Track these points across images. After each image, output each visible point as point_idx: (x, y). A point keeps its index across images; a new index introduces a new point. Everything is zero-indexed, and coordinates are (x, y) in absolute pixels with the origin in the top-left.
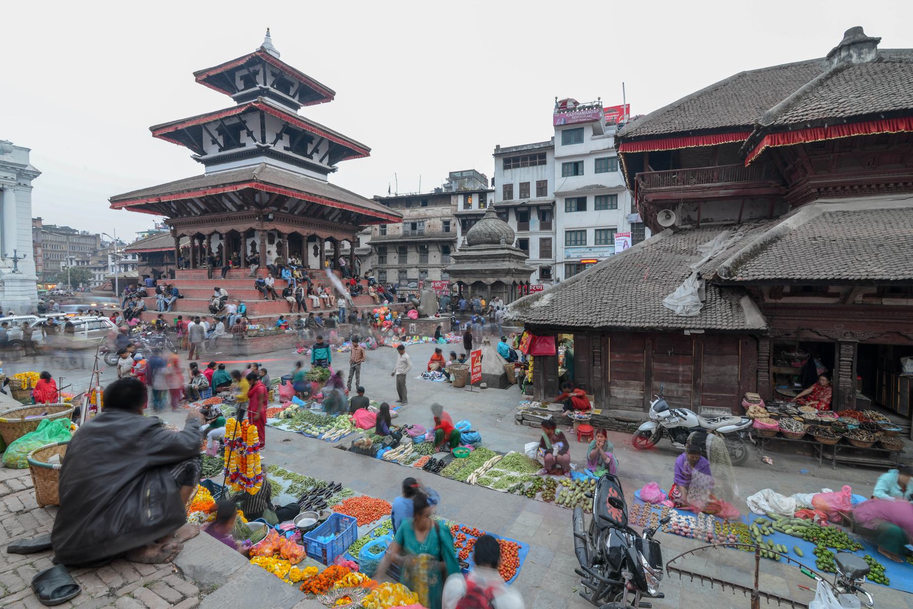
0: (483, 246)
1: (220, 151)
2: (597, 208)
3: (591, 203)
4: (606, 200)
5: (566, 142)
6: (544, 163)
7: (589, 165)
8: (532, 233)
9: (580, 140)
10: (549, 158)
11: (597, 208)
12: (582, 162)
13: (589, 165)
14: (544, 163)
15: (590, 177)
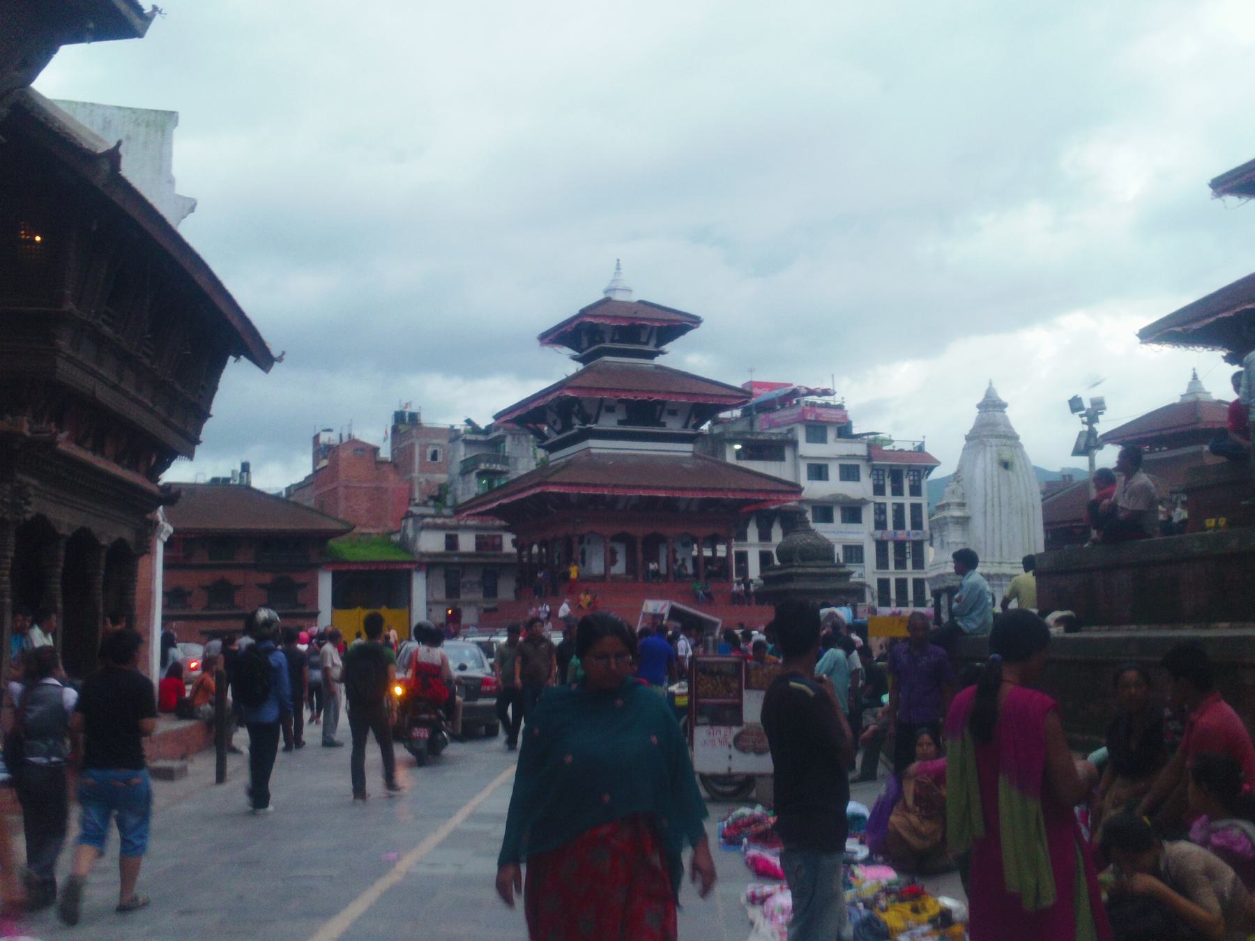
0: (820, 563)
1: (621, 423)
2: (844, 520)
3: (837, 515)
4: (853, 512)
5: (810, 439)
6: (782, 459)
7: (834, 472)
8: (751, 545)
9: (823, 440)
10: (788, 454)
11: (844, 520)
12: (826, 466)
13: (834, 472)
14: (782, 459)
15: (833, 486)
